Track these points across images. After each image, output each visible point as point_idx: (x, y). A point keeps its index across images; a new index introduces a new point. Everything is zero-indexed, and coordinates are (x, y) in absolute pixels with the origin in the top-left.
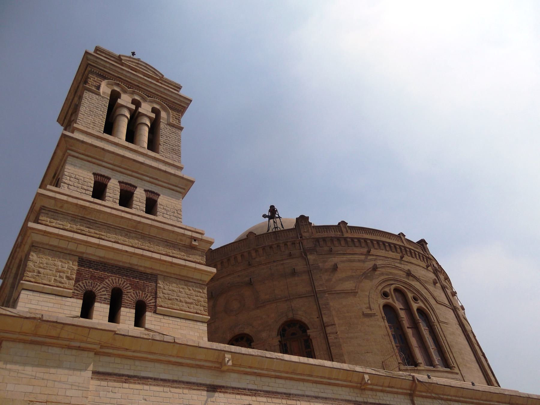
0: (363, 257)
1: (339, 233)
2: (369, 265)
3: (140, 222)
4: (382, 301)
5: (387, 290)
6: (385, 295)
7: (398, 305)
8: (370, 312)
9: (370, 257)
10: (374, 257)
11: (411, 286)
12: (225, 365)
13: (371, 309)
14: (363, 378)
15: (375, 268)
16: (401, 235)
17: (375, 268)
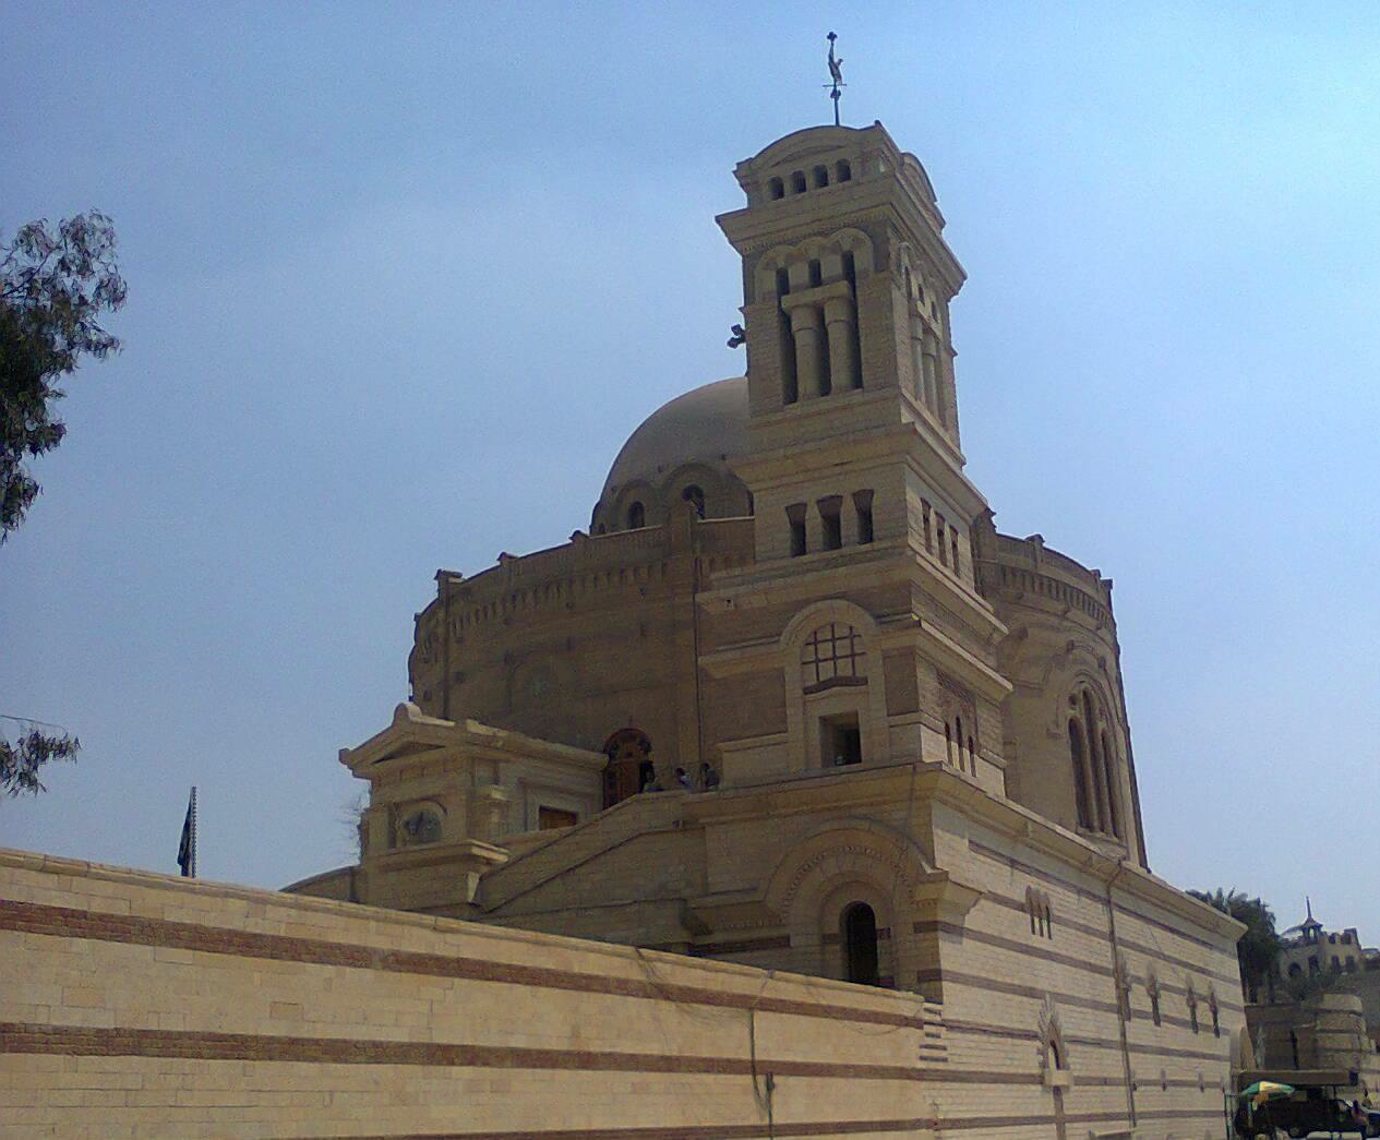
0: (1054, 621)
1: (1031, 561)
2: (1061, 640)
3: (967, 604)
4: (1071, 713)
5: (1075, 692)
6: (1073, 701)
7: (1083, 722)
8: (1056, 731)
9: (1065, 623)
10: (1070, 624)
11: (1100, 688)
12: (1027, 836)
13: (1057, 725)
14: (1090, 858)
15: (1071, 646)
16: (1097, 573)
17: (1071, 646)
